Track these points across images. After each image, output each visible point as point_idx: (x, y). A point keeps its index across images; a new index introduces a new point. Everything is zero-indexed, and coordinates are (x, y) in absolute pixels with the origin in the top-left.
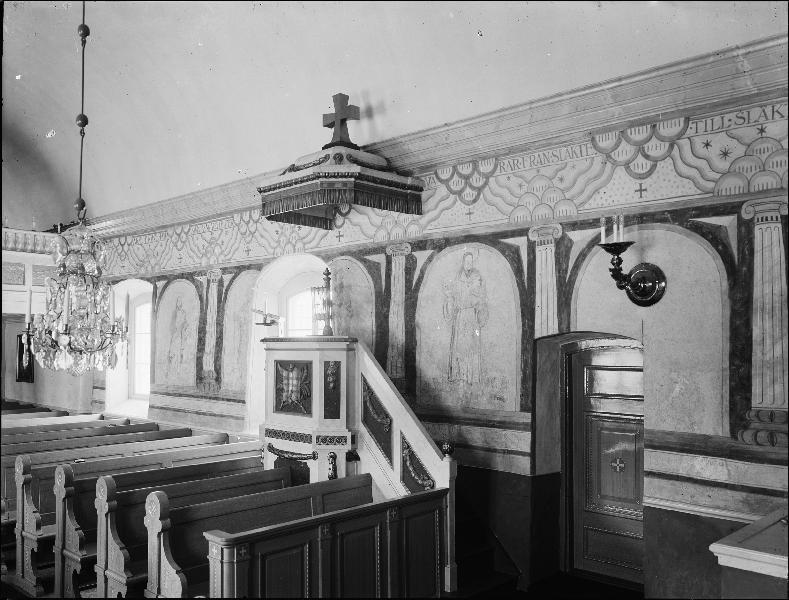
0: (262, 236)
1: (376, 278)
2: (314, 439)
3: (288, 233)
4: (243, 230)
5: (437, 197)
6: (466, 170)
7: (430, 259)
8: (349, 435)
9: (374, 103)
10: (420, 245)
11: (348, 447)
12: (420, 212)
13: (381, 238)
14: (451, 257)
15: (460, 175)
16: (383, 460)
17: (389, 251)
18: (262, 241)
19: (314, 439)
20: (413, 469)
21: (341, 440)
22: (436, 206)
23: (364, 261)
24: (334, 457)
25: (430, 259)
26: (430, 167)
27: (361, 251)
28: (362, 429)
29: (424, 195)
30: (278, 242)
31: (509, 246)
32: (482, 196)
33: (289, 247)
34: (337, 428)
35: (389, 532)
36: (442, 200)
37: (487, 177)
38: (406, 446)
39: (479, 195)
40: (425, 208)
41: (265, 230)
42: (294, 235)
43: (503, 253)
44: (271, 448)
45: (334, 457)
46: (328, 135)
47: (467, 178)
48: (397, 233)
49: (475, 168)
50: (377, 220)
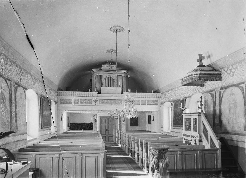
0: (190, 89)
1: (213, 97)
2: (191, 136)
5: (225, 76)
6: (230, 68)
7: (224, 92)
8: (199, 135)
9: (210, 54)
10: (222, 88)
13: (214, 87)
14: (229, 91)
16: (207, 142)
19: (191, 136)
20: (212, 143)
21: (197, 137)
23: (210, 94)
24: (196, 141)
25: (224, 92)
26: (223, 68)
27: (210, 91)
28: (203, 134)
29: (222, 75)
30: (194, 90)
31: (241, 87)
34: (196, 134)
35: (199, 156)
36: (226, 76)
37: (235, 69)
38: (211, 138)
39: (234, 74)
43: (240, 88)
44: (185, 139)
45: (196, 141)
46: (198, 64)
47: (231, 70)
48: (217, 86)
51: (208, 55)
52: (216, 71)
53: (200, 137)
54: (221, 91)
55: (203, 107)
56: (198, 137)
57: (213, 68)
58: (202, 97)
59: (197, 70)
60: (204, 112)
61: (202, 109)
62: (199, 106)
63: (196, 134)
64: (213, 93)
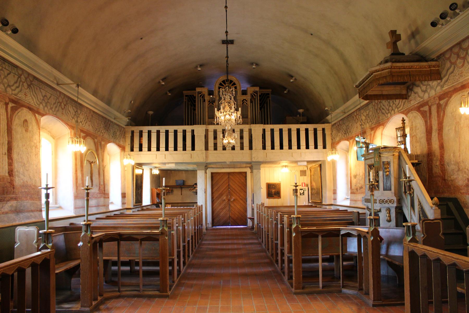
0: (383, 109)
3: (391, 105)
4: (376, 108)
8: (395, 199)
10: (441, 98)
11: (395, 205)
12: (441, 79)
15: (454, 54)
17: (430, 104)
18: (383, 111)
22: (447, 73)
30: (388, 110)
32: (466, 62)
33: (393, 112)
38: (420, 204)
39: (464, 62)
40: (442, 76)
41: (384, 105)
42: (394, 105)
49: (461, 48)
50: (424, 88)
51: (409, 32)
52: (426, 61)
53: (400, 201)
54: (442, 102)
55: (408, 139)
56: (394, 202)
57: (422, 57)
58: (403, 120)
59: (386, 61)
60: (409, 152)
61: (405, 144)
62: (399, 139)
63: (390, 195)
64: (426, 108)
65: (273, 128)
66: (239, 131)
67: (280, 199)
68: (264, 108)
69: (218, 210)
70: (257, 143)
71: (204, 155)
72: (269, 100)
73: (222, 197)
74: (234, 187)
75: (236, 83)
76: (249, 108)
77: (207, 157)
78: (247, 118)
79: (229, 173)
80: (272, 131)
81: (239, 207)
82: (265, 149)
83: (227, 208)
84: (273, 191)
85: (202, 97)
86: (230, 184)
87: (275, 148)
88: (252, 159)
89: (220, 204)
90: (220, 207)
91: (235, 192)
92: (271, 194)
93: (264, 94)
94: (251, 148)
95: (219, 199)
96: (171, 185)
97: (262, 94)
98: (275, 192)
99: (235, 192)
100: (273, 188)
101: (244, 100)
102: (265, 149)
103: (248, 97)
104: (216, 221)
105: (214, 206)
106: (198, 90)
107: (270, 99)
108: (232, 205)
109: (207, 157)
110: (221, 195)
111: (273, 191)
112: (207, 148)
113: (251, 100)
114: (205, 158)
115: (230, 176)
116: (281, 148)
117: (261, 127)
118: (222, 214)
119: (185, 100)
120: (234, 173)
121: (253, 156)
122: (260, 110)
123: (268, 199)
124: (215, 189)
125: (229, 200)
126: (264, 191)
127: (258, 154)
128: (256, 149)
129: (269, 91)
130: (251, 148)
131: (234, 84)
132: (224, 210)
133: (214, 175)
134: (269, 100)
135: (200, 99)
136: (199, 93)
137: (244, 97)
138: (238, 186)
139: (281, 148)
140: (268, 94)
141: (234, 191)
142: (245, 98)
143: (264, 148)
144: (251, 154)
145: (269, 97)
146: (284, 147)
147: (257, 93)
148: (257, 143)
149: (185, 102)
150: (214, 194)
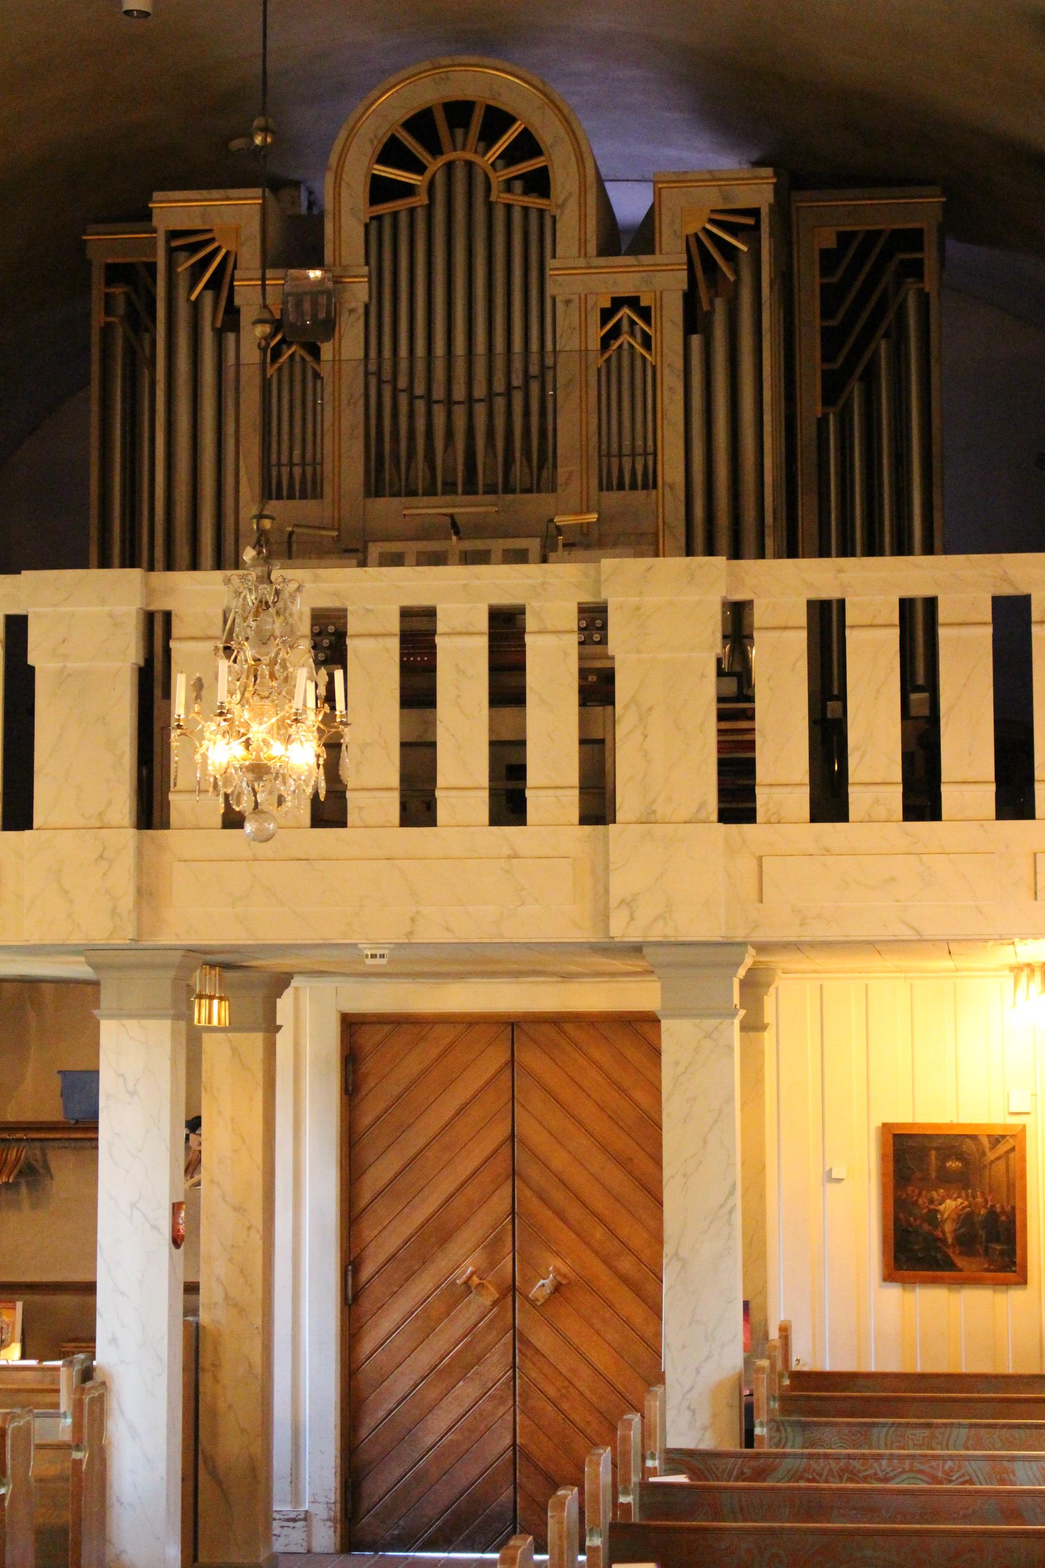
65: (919, 590)
66: (483, 623)
67: (1016, 1295)
68: (870, 378)
69: (400, 1384)
70: (667, 748)
71: (123, 879)
72: (924, 300)
73: (443, 1262)
74: (559, 1160)
75: (549, 132)
76: (671, 382)
77: (147, 892)
78: (650, 482)
79: (513, 1027)
80: (826, 623)
81: (602, 1358)
82: (748, 816)
83: (495, 1366)
84: (950, 1206)
85: (215, 284)
86: (500, 1138)
87: (857, 798)
88: (604, 917)
89: (425, 1323)
90: (424, 1358)
91: (575, 1212)
92: (934, 1243)
93: (872, 236)
94: (597, 805)
95: (410, 1276)
96: (29, 1116)
97: (845, 238)
98: (966, 1219)
99: (575, 1212)
100: (946, 1179)
101: (618, 303)
102: (748, 816)
103: (661, 280)
104: (378, 1486)
105: (367, 1345)
106: (174, 210)
107: (930, 285)
108: (542, 1338)
109: (147, 892)
110: (437, 1234)
111: (950, 1206)
112: (150, 809)
113: (690, 299)
114: (127, 902)
115: (530, 1058)
116: (922, 798)
117: (714, 579)
118: (439, 1422)
119: (98, 319)
120: (557, 1021)
121: (618, 889)
122: (832, 389)
123: (894, 1292)
124: (377, 1175)
125: (511, 1290)
126: (855, 1211)
127: (678, 866)
128: (645, 821)
129: (921, 209)
130: (597, 805)
131: (527, 146)
132: (466, 1391)
133: (369, 1039)
134: (924, 300)
135: (196, 307)
136: (188, 242)
137: (624, 276)
138: (604, 1148)
139: (922, 798)
140: (913, 239)
141: (558, 1196)
142: (626, 287)
143: (737, 801)
144: (601, 873)
145: (915, 269)
146: (948, 793)
147: (750, 234)
148: (667, 748)
149: (107, 330)
150: (368, 1230)
